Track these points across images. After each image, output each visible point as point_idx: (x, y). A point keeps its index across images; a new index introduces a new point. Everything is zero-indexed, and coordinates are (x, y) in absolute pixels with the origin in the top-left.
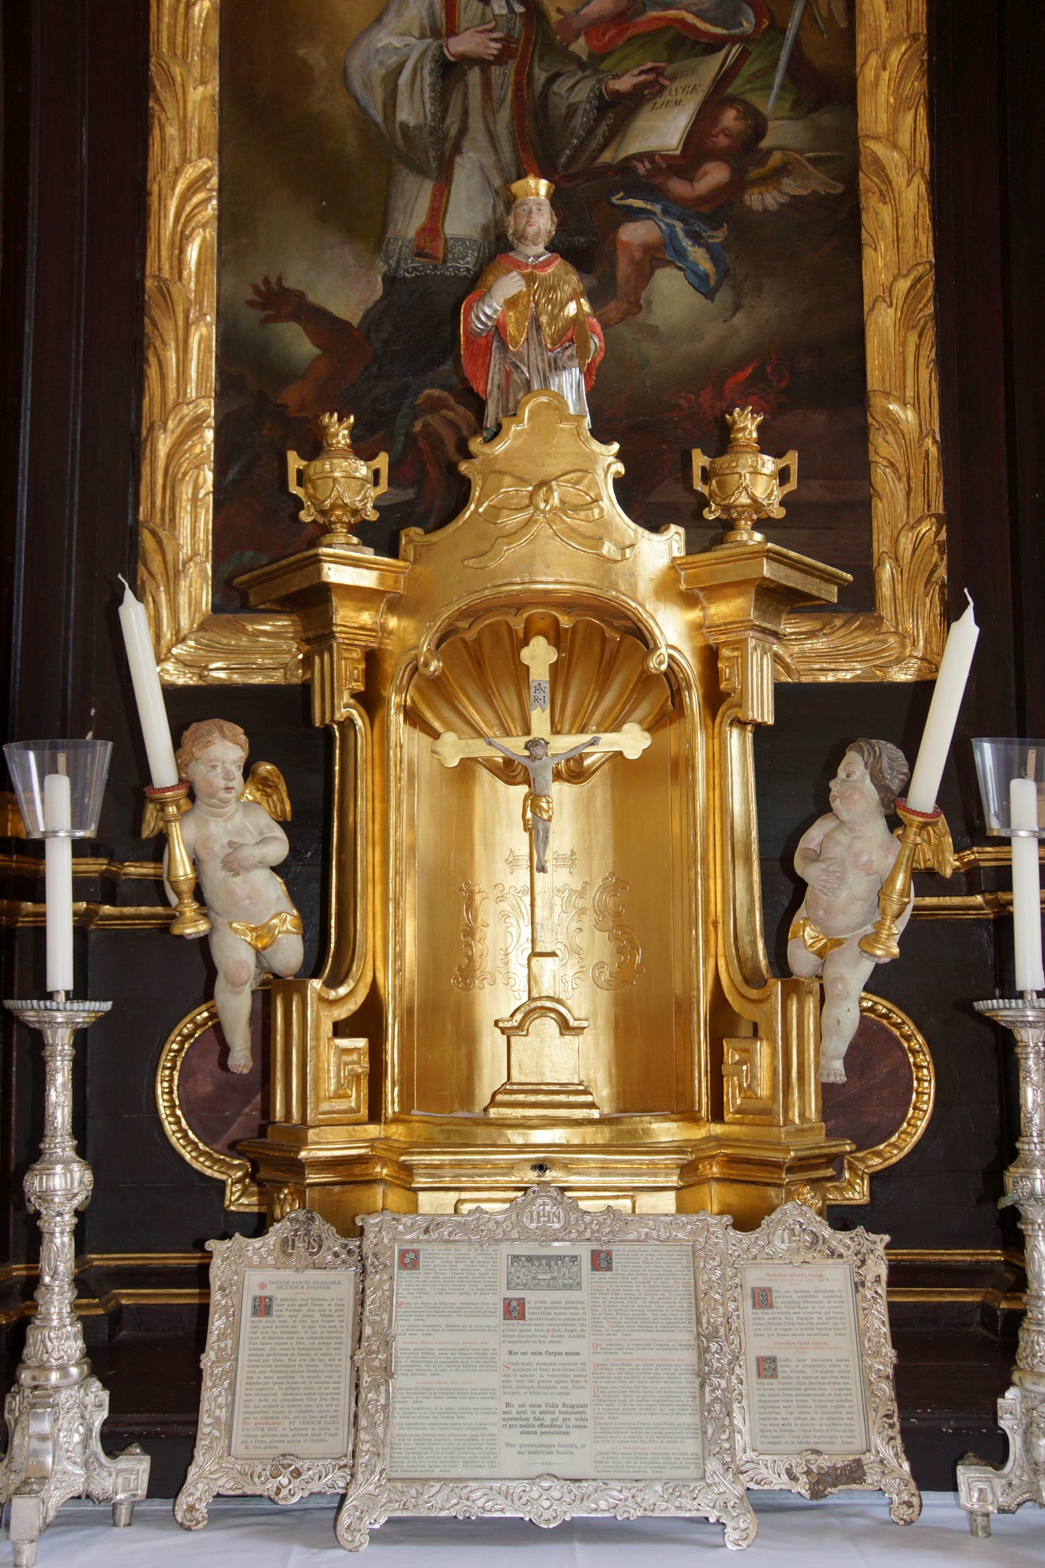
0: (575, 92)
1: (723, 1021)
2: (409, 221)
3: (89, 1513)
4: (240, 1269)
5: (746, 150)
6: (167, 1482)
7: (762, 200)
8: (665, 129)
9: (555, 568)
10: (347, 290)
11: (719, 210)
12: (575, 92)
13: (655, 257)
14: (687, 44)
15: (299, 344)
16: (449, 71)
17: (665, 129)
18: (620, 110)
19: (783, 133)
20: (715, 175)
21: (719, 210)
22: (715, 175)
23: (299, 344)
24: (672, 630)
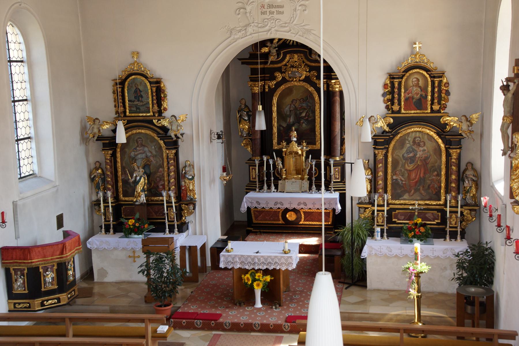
0: (298, 112)
1: (303, 171)
2: (288, 121)
3: (274, 192)
4: (280, 182)
5: (308, 116)
6: (277, 191)
7: (309, 119)
8: (304, 115)
9: (295, 150)
10: (285, 125)
11: (307, 120)
12: (298, 112)
13: (303, 123)
14: (305, 109)
15: (282, 128)
16: (290, 111)
17: (304, 115)
18: (301, 113)
19: (311, 115)
20: (307, 117)
21: (307, 120)
22: (307, 117)
23: (282, 128)
24: (300, 152)
